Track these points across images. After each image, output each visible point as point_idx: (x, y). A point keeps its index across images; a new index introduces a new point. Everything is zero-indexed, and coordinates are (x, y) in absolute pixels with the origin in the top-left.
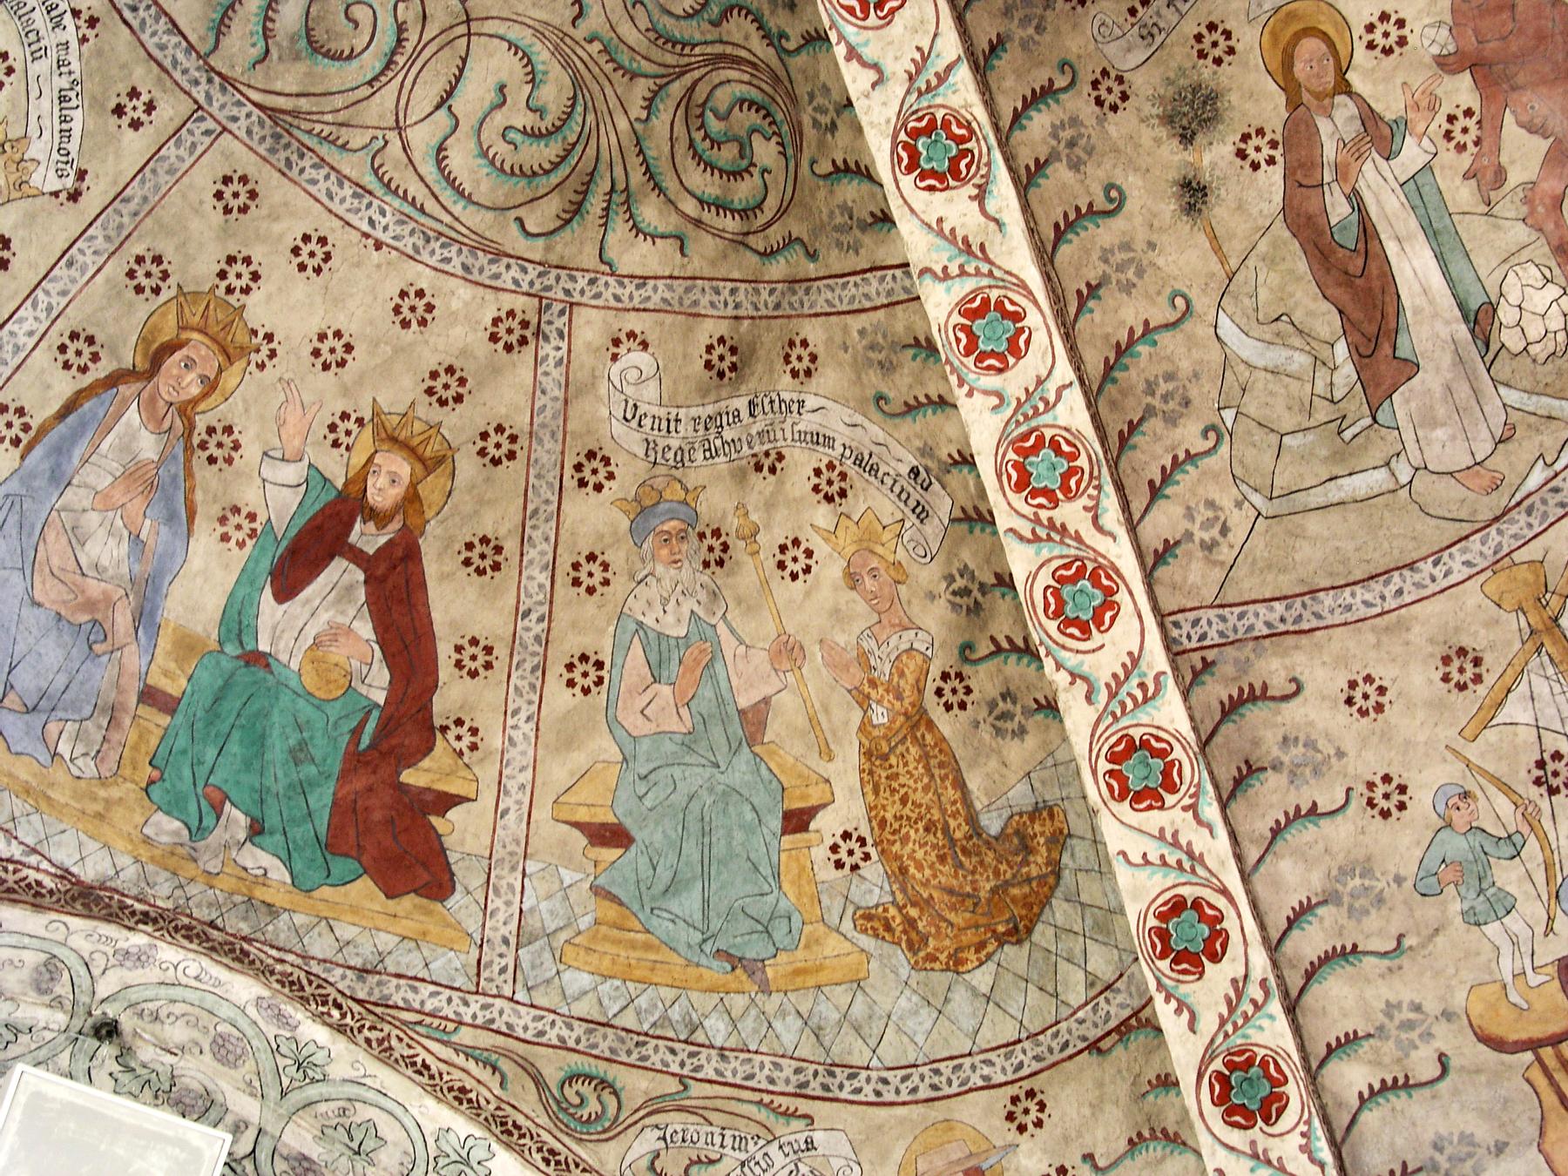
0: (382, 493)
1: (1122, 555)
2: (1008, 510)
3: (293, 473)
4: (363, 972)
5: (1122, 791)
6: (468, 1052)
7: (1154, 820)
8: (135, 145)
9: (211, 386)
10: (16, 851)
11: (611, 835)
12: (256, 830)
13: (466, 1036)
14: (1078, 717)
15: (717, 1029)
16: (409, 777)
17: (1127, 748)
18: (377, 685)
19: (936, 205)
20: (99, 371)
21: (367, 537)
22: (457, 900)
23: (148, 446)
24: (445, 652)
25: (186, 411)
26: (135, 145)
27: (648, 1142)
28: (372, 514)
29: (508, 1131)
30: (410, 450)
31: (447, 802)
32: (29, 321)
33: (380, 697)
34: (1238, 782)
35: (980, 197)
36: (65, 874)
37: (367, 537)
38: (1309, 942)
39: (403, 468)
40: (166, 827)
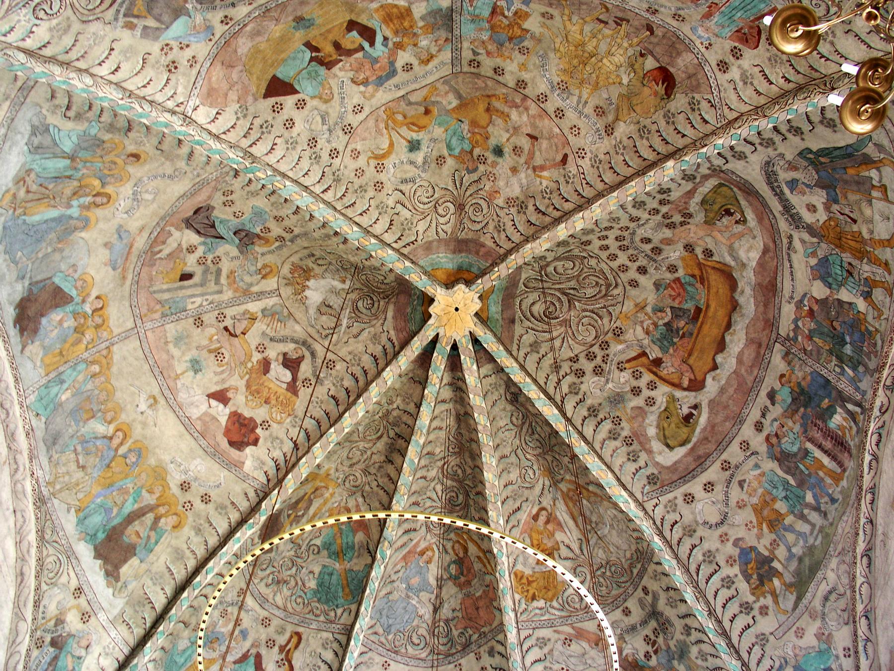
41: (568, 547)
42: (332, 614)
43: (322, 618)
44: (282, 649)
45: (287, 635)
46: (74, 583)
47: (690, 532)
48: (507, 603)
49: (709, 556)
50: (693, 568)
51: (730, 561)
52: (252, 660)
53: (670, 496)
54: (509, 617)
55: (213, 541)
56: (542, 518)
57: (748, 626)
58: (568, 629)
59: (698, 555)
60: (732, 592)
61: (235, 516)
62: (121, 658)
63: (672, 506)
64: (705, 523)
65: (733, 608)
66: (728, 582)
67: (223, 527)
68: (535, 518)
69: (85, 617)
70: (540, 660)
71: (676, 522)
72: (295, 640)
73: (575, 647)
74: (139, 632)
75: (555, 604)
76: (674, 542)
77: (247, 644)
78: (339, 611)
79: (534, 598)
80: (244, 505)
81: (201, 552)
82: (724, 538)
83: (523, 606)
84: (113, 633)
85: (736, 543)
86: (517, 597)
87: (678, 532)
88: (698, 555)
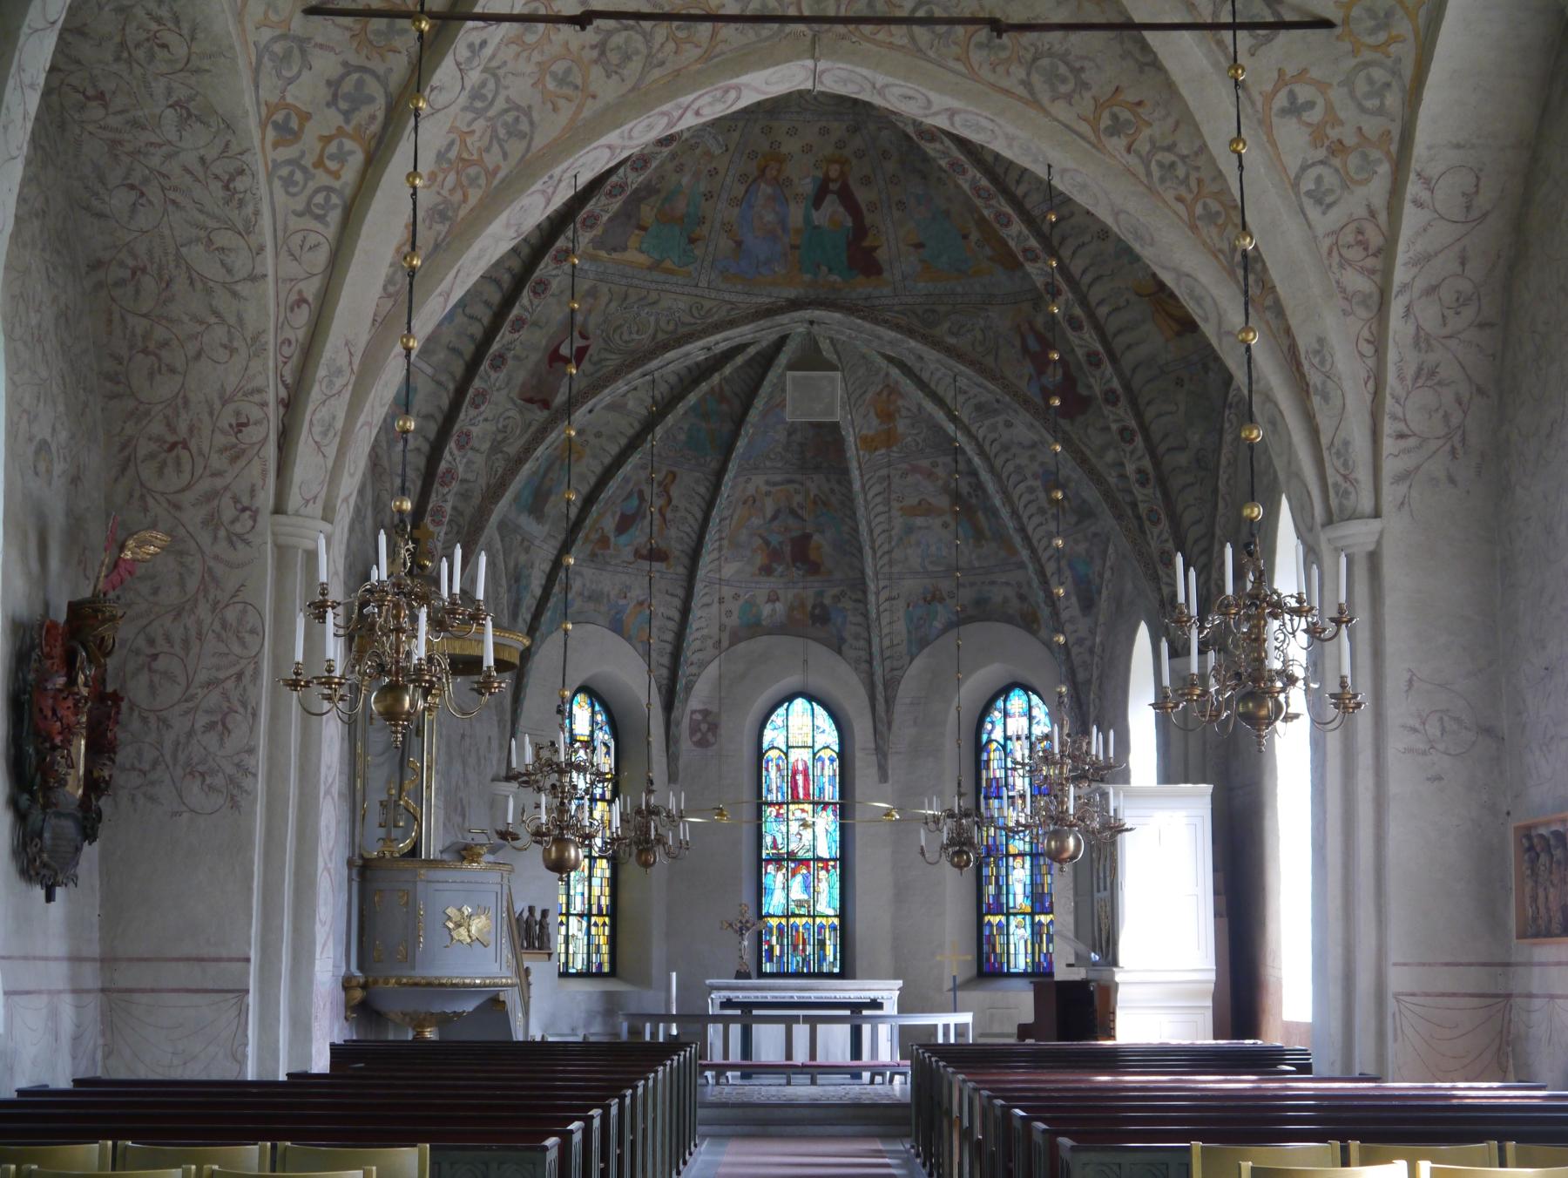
0: (834, 173)
1: (1009, 210)
2: (979, 202)
3: (808, 180)
4: (866, 299)
5: (1028, 260)
6: (897, 312)
7: (1038, 265)
8: (736, 135)
9: (779, 171)
10: (773, 300)
11: (919, 246)
12: (830, 270)
13: (896, 308)
14: (1012, 244)
15: (959, 289)
16: (866, 244)
17: (1025, 251)
18: (849, 222)
19: (932, 145)
20: (750, 180)
21: (833, 186)
22: (886, 275)
23: (769, 190)
24: (863, 207)
25: (776, 179)
26: (736, 135)
27: (946, 325)
28: (833, 181)
29: (910, 332)
30: (836, 162)
31: (876, 248)
32: (728, 180)
33: (850, 224)
34: (1061, 244)
35: (942, 143)
36: (788, 300)
37: (833, 186)
38: (1087, 279)
39: (837, 167)
40: (807, 277)
41: (909, 410)
42: (702, 461)
43: (693, 462)
44: (660, 484)
45: (664, 473)
46: (519, 538)
47: (1006, 448)
48: (851, 452)
49: (1019, 469)
50: (1004, 476)
51: (1035, 476)
52: (636, 495)
53: (992, 420)
54: (854, 465)
55: (607, 460)
56: (885, 393)
57: (1041, 524)
58: (904, 466)
59: (1010, 467)
60: (1032, 497)
61: (623, 441)
62: (553, 557)
63: (994, 428)
64: (1020, 444)
65: (1032, 508)
66: (1031, 490)
67: (614, 450)
68: (880, 394)
69: (527, 550)
70: (880, 494)
71: (995, 440)
72: (670, 477)
73: (910, 479)
74: (561, 537)
75: (895, 449)
76: (992, 455)
77: (631, 485)
78: (708, 459)
79: (876, 449)
80: (631, 432)
81: (598, 470)
82: (1032, 458)
83: (867, 457)
84: (545, 547)
85: (1042, 464)
86: (861, 453)
87: (996, 447)
88: (1010, 467)
